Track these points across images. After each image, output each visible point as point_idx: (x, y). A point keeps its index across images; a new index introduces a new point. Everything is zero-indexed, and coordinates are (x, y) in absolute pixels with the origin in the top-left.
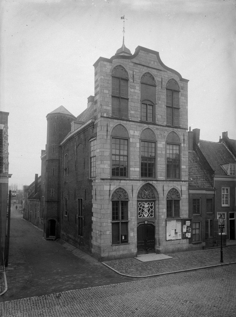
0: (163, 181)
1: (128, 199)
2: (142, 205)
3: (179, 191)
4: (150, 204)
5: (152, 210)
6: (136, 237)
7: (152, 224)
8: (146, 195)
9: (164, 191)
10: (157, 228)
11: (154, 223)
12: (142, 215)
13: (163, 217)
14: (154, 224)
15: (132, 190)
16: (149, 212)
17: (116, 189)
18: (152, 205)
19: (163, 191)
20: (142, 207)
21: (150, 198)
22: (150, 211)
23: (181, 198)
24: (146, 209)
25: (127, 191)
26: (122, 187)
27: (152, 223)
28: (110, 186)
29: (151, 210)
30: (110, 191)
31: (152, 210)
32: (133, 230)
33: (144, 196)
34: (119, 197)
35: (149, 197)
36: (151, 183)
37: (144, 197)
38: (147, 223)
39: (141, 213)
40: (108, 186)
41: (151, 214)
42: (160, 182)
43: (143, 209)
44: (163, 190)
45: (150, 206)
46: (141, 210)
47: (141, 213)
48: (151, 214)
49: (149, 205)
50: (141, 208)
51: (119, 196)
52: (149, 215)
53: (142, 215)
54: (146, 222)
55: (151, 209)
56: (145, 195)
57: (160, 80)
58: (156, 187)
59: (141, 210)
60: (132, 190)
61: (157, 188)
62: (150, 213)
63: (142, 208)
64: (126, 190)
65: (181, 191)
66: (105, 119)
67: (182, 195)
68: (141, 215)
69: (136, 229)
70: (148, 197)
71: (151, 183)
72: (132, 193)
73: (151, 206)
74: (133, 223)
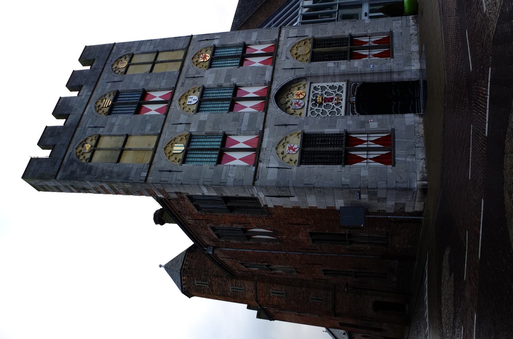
0: (274, 69)
2: (317, 108)
4: (316, 92)
5: (330, 87)
6: (380, 117)
7: (359, 88)
8: (297, 101)
10: (368, 79)
11: (356, 85)
12: (336, 107)
14: (358, 84)
18: (319, 87)
20: (321, 109)
21: (304, 94)
27: (357, 87)
29: (328, 90)
30: (278, 168)
31: (328, 88)
32: (363, 124)
33: (299, 105)
34: (294, 150)
35: (302, 95)
37: (300, 104)
39: (332, 109)
41: (337, 90)
42: (276, 75)
43: (324, 105)
45: (320, 93)
46: (327, 110)
47: (332, 109)
48: (337, 90)
49: (319, 94)
50: (323, 110)
52: (339, 93)
53: (338, 107)
54: (353, 99)
55: (326, 90)
56: (297, 103)
57: (110, 84)
59: (327, 110)
62: (335, 92)
63: (323, 108)
66: (150, 174)
68: (337, 109)
69: (362, 118)
70: (301, 97)
72: (289, 126)
73: (320, 90)
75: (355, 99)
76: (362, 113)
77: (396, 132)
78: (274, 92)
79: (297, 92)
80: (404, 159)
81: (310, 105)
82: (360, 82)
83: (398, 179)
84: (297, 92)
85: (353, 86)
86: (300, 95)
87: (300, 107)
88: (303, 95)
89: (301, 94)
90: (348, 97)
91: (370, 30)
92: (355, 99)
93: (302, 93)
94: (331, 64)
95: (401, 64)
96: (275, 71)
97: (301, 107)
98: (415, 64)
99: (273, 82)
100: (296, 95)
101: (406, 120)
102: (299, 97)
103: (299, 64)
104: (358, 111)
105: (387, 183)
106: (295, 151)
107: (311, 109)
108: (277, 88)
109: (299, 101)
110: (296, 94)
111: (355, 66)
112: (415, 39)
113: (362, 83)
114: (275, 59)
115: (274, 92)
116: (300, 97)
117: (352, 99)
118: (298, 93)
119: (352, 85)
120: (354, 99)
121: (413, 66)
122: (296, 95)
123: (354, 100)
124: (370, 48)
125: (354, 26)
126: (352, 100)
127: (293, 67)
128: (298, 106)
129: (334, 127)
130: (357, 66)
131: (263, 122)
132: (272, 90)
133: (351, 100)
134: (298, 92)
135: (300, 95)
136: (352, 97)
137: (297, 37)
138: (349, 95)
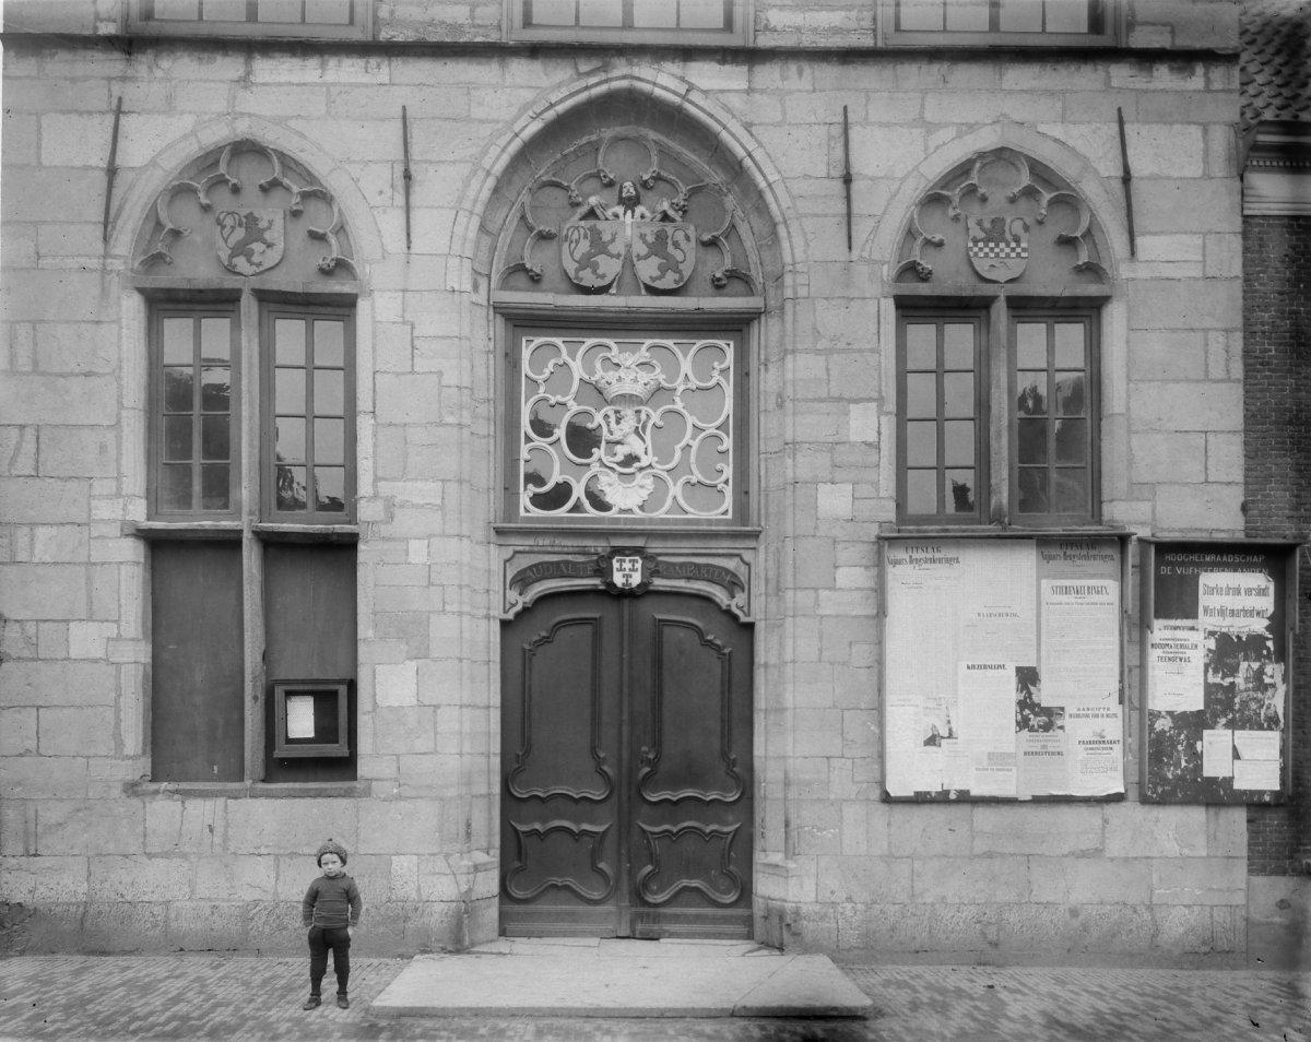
1: (341, 267)
3: (1090, 190)
9: (855, 186)
11: (733, 584)
13: (835, 501)
14: (740, 598)
15: (407, 176)
16: (664, 454)
17: (192, 149)
19: (838, 186)
22: (686, 439)
23: (1125, 271)
24: (629, 423)
25: (334, 183)
26: (270, 137)
28: (110, 119)
33: (586, 262)
34: (241, 249)
35: (663, 270)
36: (673, 84)
38: (636, 579)
40: (97, 119)
44: (847, 180)
51: (240, 233)
58: (736, 139)
60: (407, 176)
61: (751, 146)
64: (319, 166)
65: (1127, 179)
67: (1139, 241)
71: (673, 84)
72: (400, 199)
74: (418, 552)
75: (627, 584)
78: (663, 79)
79: (688, 238)
82: (749, 610)
84: (688, 238)
85: (727, 571)
86: (655, 261)
87: (571, 267)
88: (659, 278)
89: (670, 265)
90: (639, 542)
92: (627, 584)
93: (680, 272)
97: (572, 274)
102: (644, 250)
106: (231, 256)
108: (694, 96)
109: (618, 256)
110: (670, 233)
113: (743, 619)
115: (662, 81)
116: (646, 257)
117: (627, 565)
118: (676, 245)
119: (731, 564)
120: (628, 576)
123: (618, 579)
126: (616, 565)
128: (577, 256)
133: (621, 561)
134: (683, 244)
136: (639, 565)
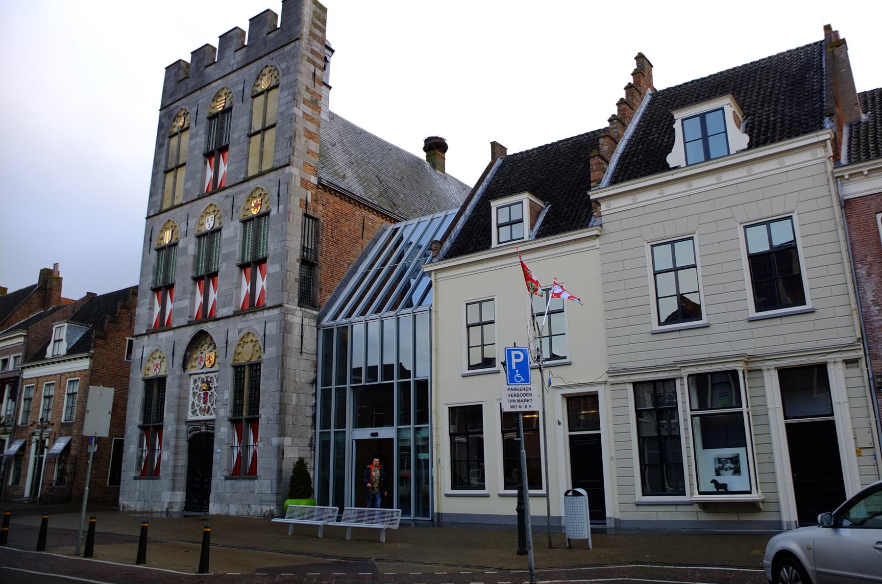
2: (200, 385)
8: (204, 360)
45: (213, 386)
71: (205, 327)
76: (190, 441)
77: (157, 481)
80: (137, 489)
81: (203, 376)
83: (125, 482)
86: (209, 361)
91: (261, 446)
94: (228, 395)
95: (217, 490)
96: (226, 320)
98: (215, 507)
99: (215, 322)
100: (210, 356)
101: (166, 492)
103: (231, 351)
104: (195, 436)
105: (124, 471)
107: (199, 378)
111: (222, 428)
112: (243, 511)
114: (239, 315)
121: (214, 506)
122: (210, 356)
124: (247, 447)
125: (271, 421)
127: (228, 343)
129: (167, 412)
130: (221, 430)
131: (179, 325)
132: (206, 324)
135: (209, 361)
137: (265, 336)
138: (208, 423)
